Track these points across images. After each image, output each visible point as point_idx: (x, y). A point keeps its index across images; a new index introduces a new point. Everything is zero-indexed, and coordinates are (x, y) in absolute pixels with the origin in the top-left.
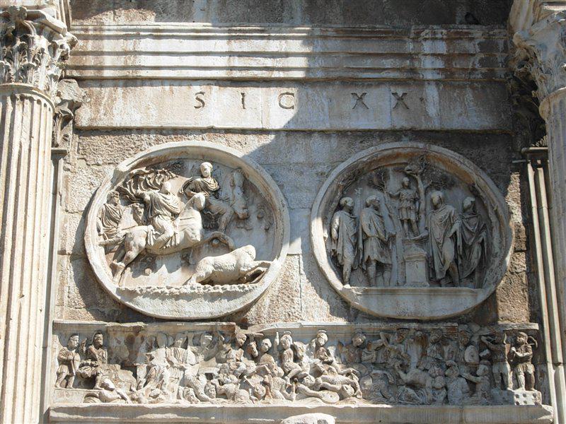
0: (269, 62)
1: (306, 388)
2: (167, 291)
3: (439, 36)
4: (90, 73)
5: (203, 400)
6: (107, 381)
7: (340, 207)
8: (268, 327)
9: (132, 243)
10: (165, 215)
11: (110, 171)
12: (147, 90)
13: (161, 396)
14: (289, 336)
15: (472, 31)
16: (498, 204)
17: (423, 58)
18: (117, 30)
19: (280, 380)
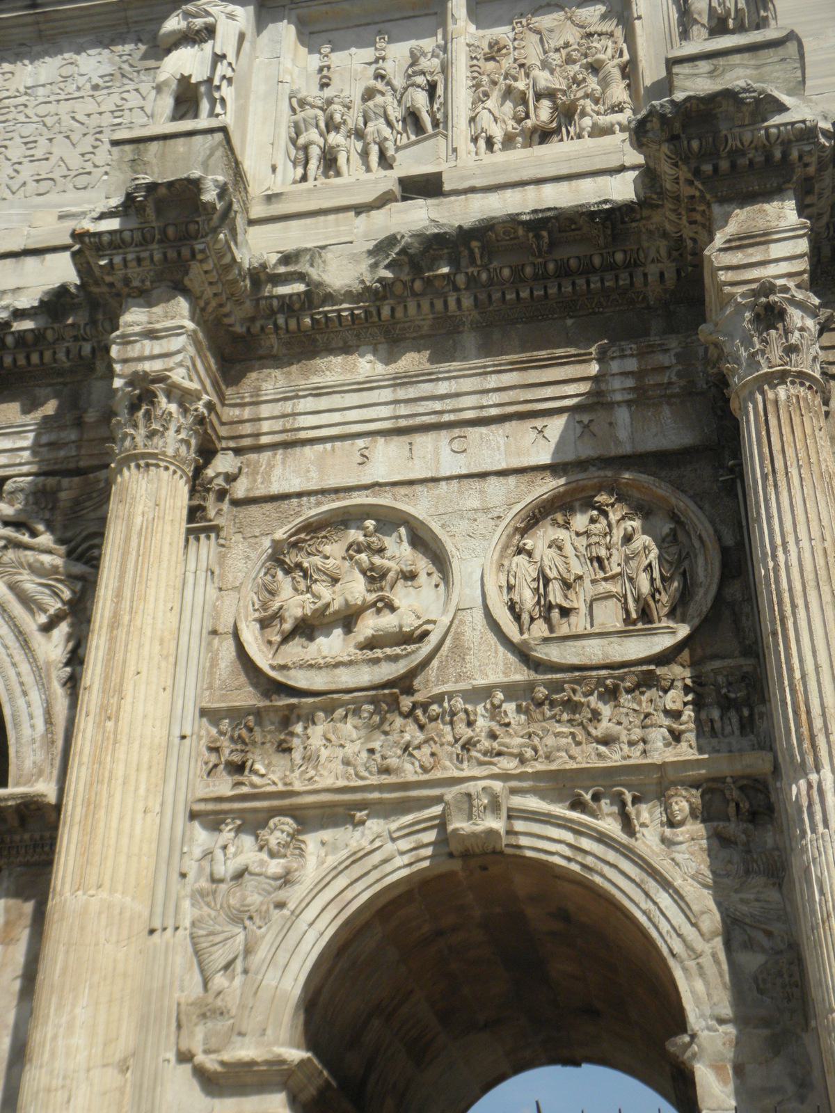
0: (438, 406)
1: (479, 755)
2: (322, 661)
3: (628, 352)
4: (246, 442)
5: (362, 778)
6: (258, 766)
7: (520, 551)
8: (436, 690)
9: (287, 615)
10: (324, 581)
11: (267, 543)
12: (307, 450)
13: (316, 778)
14: (460, 699)
15: (666, 342)
16: (700, 526)
17: (610, 379)
18: (274, 394)
19: (449, 748)
